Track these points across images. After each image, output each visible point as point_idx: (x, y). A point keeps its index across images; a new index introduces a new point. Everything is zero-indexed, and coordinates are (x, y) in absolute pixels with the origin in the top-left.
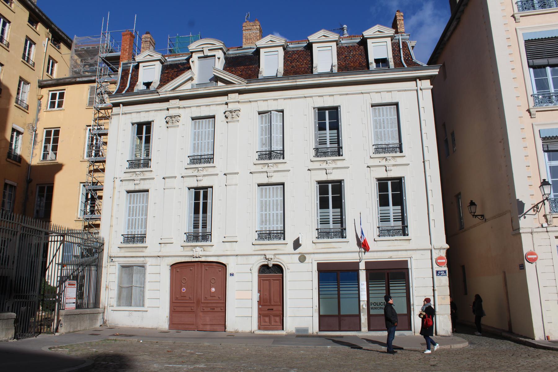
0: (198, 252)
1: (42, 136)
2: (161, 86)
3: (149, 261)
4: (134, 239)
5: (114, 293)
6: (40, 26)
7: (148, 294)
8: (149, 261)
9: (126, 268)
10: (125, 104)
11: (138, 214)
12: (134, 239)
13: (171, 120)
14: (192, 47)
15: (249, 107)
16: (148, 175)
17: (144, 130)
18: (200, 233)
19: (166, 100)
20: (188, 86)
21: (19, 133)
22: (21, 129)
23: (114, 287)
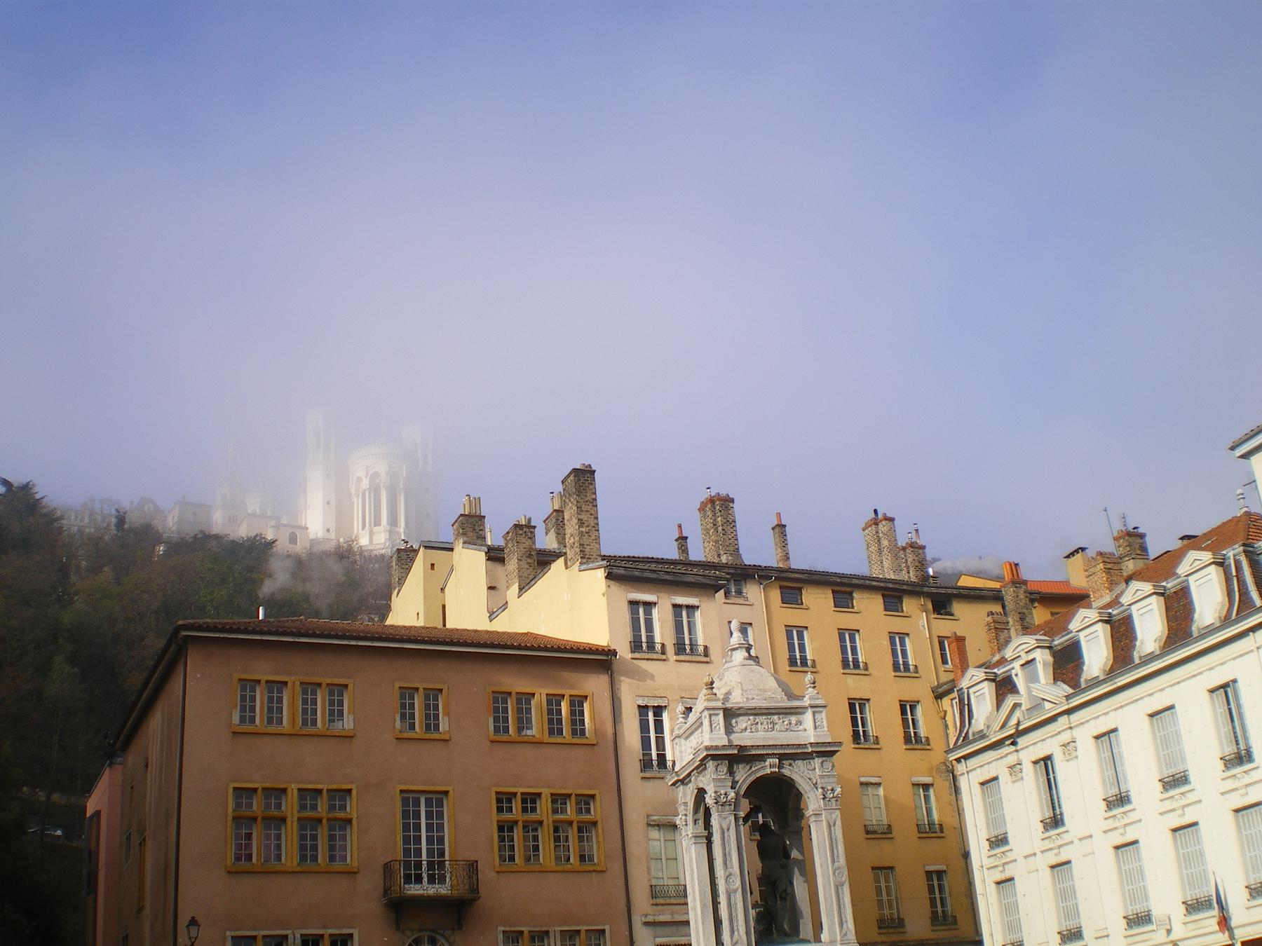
10: (966, 757)
13: (1014, 768)
16: (1010, 856)
22: (928, 780)
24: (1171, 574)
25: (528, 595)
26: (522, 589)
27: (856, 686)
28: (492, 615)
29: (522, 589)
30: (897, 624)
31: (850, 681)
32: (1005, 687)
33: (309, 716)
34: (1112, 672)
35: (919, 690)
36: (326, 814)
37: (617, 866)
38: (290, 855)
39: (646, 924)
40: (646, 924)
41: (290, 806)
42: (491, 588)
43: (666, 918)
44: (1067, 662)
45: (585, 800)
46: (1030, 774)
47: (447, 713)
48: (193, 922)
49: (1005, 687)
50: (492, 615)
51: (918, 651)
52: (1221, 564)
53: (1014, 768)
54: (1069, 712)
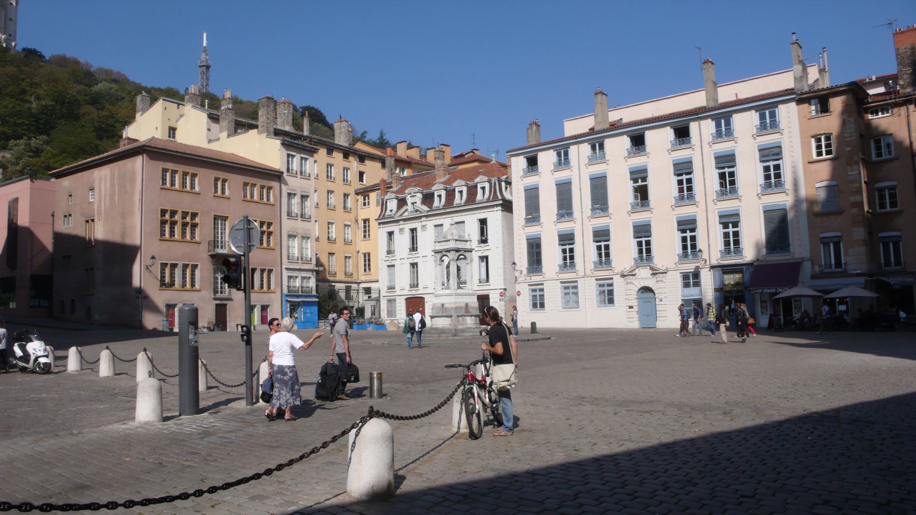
0: (414, 292)
1: (361, 224)
2: (397, 211)
3: (397, 298)
4: (391, 288)
5: (386, 312)
6: (351, 158)
7: (398, 312)
8: (397, 298)
9: (389, 301)
11: (392, 277)
12: (391, 288)
13: (401, 230)
14: (407, 191)
15: (430, 223)
17: (391, 234)
18: (414, 285)
19: (398, 221)
20: (406, 214)
21: (349, 226)
23: (386, 309)
24: (472, 179)
25: (232, 139)
26: (229, 136)
27: (331, 186)
28: (210, 141)
29: (229, 136)
30: (346, 164)
31: (329, 183)
32: (402, 203)
33: (184, 184)
34: (445, 207)
35: (351, 190)
36: (190, 222)
37: (278, 248)
38: (177, 236)
39: (287, 269)
40: (287, 269)
41: (177, 217)
42: (209, 130)
43: (291, 267)
44: (428, 199)
45: (270, 224)
46: (407, 234)
47: (229, 188)
48: (153, 258)
49: (402, 203)
50: (210, 141)
51: (352, 176)
52: (489, 182)
53: (401, 230)
54: (426, 216)
